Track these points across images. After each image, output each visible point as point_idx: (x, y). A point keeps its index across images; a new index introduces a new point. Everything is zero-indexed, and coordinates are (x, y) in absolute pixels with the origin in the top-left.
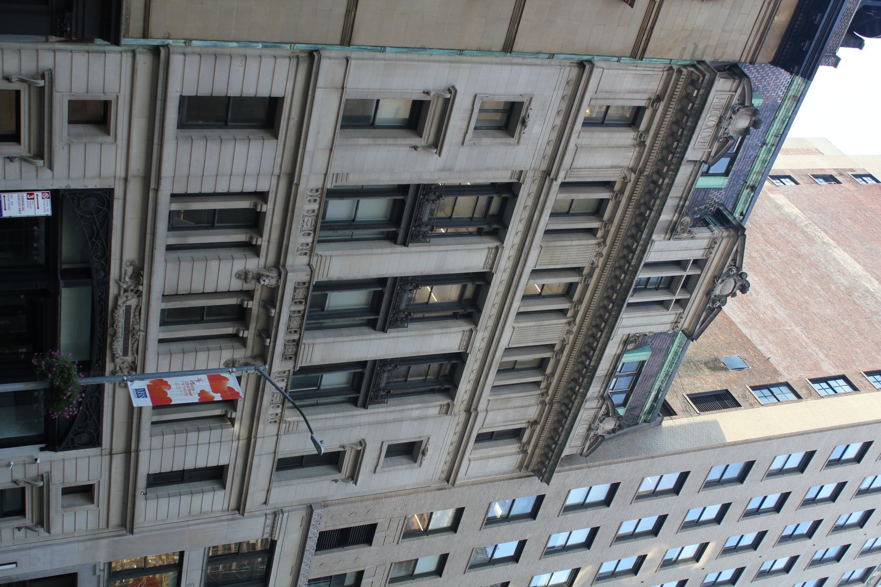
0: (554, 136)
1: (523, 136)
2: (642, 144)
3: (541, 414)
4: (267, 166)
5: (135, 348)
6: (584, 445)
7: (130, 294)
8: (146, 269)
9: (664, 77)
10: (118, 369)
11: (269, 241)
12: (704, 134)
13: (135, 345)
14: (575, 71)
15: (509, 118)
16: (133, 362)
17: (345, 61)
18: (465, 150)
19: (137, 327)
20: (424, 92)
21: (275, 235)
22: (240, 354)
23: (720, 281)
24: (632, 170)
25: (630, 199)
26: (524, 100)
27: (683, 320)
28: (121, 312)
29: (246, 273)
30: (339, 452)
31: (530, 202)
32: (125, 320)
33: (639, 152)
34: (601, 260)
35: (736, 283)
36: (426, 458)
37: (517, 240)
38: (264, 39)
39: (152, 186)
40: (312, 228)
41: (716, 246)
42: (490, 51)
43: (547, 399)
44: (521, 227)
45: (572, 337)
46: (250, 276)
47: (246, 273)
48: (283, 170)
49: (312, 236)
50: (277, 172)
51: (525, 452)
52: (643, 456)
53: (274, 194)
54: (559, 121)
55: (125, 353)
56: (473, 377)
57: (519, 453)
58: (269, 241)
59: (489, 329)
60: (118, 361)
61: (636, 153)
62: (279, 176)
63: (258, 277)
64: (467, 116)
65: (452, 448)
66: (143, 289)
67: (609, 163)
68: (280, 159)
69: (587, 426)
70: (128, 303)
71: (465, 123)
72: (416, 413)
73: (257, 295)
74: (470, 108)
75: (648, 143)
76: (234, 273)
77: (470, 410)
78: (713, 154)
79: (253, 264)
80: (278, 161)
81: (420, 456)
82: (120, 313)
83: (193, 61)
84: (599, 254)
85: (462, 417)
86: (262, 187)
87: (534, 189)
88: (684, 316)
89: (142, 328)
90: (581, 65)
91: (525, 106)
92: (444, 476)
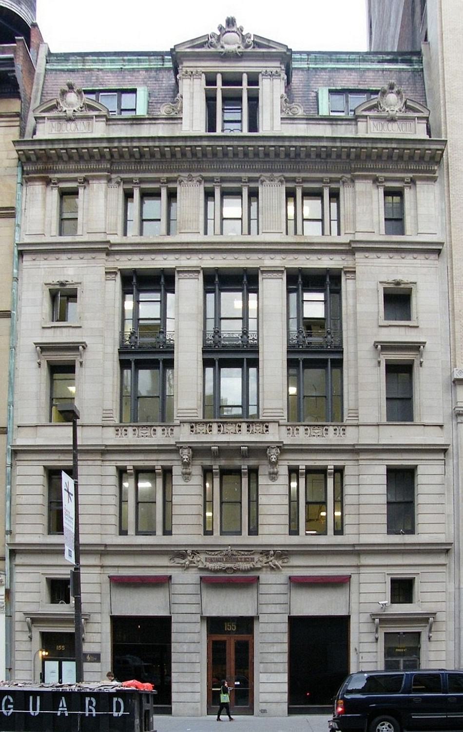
0: (76, 256)
1: (75, 280)
2: (86, 180)
3: (365, 177)
4: (96, 470)
5: (246, 553)
6: (413, 119)
7: (195, 559)
8: (173, 549)
9: (32, 184)
10: (267, 564)
11: (158, 460)
12: (82, 128)
13: (242, 553)
14: (26, 258)
15: (62, 297)
16: (261, 553)
17: (20, 428)
18: (86, 324)
19: (225, 553)
20: (40, 367)
21: (154, 457)
22: (264, 470)
23: (222, 50)
24: (109, 180)
25: (137, 171)
26: (47, 288)
27: (268, 70)
28: (211, 565)
29: (184, 474)
30: (387, 366)
31: (136, 257)
32: (218, 561)
33: (93, 180)
34: (194, 174)
35: (226, 32)
36: (405, 280)
37: (171, 257)
38: (4, 485)
39: (103, 548)
40: (149, 428)
41: (189, 70)
42: (12, 326)
43: (349, 176)
44: (159, 257)
45: (276, 175)
46: (184, 470)
47: (184, 474)
48: (98, 458)
49: (155, 428)
50: (99, 463)
51: (413, 181)
52: (439, 47)
53: (118, 462)
54: (64, 256)
55: (253, 560)
56: (314, 257)
57: (415, 184)
58: (158, 460)
59: (260, 256)
60: (259, 566)
61: (94, 182)
62: (103, 461)
63: (186, 465)
64: (58, 330)
65: (396, 256)
66: (189, 550)
67: (102, 201)
68: (89, 462)
69: (390, 125)
70: (203, 560)
71: (64, 329)
72: (351, 301)
73: (207, 463)
74: (53, 329)
75: (83, 175)
76: (185, 483)
77: (351, 249)
78: (96, 113)
79: (177, 470)
80: (90, 463)
81: (402, 286)
82: (210, 565)
83: (18, 529)
84: (190, 179)
85: (358, 255)
86: (113, 471)
87: (124, 258)
88: (264, 70)
89: (226, 549)
90: (21, 254)
91: (52, 287)
92: (433, 256)
